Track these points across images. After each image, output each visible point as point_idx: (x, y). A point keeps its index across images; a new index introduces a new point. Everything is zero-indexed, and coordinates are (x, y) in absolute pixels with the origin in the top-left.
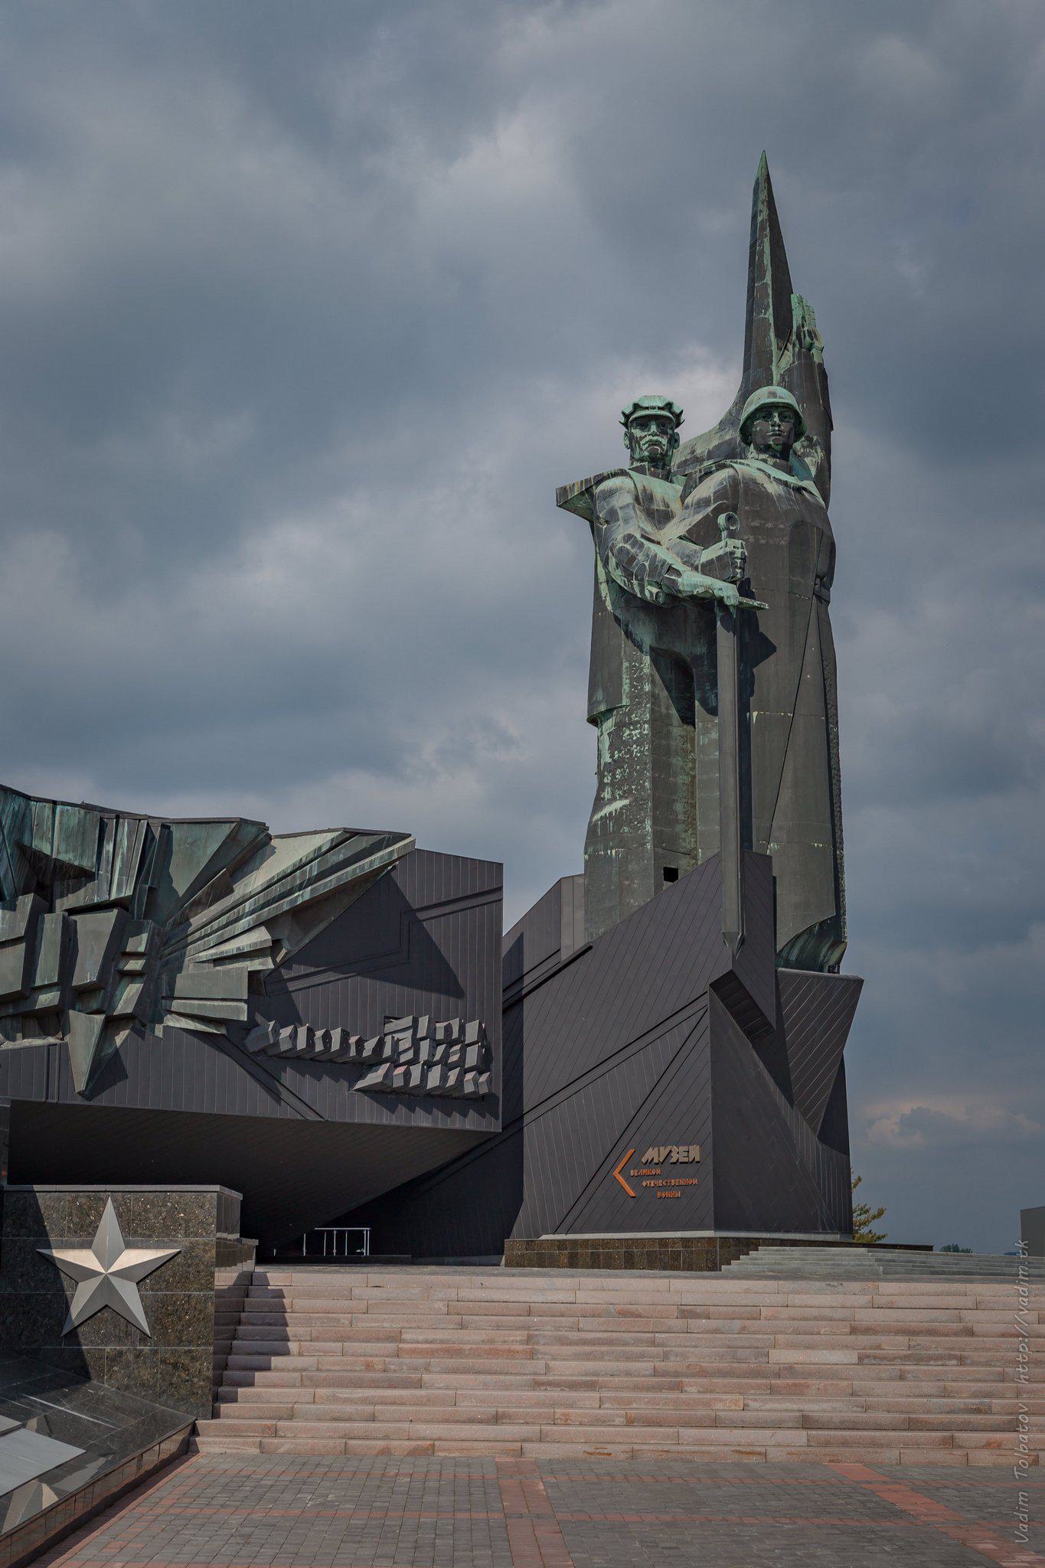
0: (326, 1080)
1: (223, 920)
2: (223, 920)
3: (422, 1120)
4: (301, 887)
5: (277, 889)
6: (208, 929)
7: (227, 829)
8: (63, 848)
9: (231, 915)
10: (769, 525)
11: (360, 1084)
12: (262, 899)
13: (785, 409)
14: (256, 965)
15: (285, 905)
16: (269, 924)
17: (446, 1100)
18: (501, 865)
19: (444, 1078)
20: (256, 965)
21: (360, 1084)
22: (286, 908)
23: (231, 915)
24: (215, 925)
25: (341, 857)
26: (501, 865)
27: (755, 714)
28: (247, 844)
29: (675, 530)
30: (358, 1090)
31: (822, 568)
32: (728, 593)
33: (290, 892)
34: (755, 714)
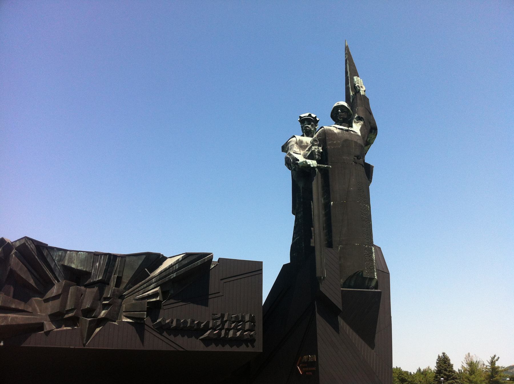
0: (186, 337)
1: (145, 285)
2: (145, 285)
3: (227, 348)
4: (173, 273)
5: (164, 274)
6: (140, 289)
7: (144, 256)
8: (79, 265)
9: (148, 284)
10: (335, 142)
11: (201, 338)
12: (158, 277)
15: (167, 279)
16: (161, 286)
17: (237, 341)
18: (262, 262)
19: (235, 333)
21: (201, 338)
22: (167, 280)
23: (148, 284)
24: (142, 287)
25: (186, 262)
26: (262, 262)
27: (332, 203)
28: (154, 260)
30: (202, 340)
31: (358, 153)
32: (313, 163)
33: (169, 274)
34: (332, 203)
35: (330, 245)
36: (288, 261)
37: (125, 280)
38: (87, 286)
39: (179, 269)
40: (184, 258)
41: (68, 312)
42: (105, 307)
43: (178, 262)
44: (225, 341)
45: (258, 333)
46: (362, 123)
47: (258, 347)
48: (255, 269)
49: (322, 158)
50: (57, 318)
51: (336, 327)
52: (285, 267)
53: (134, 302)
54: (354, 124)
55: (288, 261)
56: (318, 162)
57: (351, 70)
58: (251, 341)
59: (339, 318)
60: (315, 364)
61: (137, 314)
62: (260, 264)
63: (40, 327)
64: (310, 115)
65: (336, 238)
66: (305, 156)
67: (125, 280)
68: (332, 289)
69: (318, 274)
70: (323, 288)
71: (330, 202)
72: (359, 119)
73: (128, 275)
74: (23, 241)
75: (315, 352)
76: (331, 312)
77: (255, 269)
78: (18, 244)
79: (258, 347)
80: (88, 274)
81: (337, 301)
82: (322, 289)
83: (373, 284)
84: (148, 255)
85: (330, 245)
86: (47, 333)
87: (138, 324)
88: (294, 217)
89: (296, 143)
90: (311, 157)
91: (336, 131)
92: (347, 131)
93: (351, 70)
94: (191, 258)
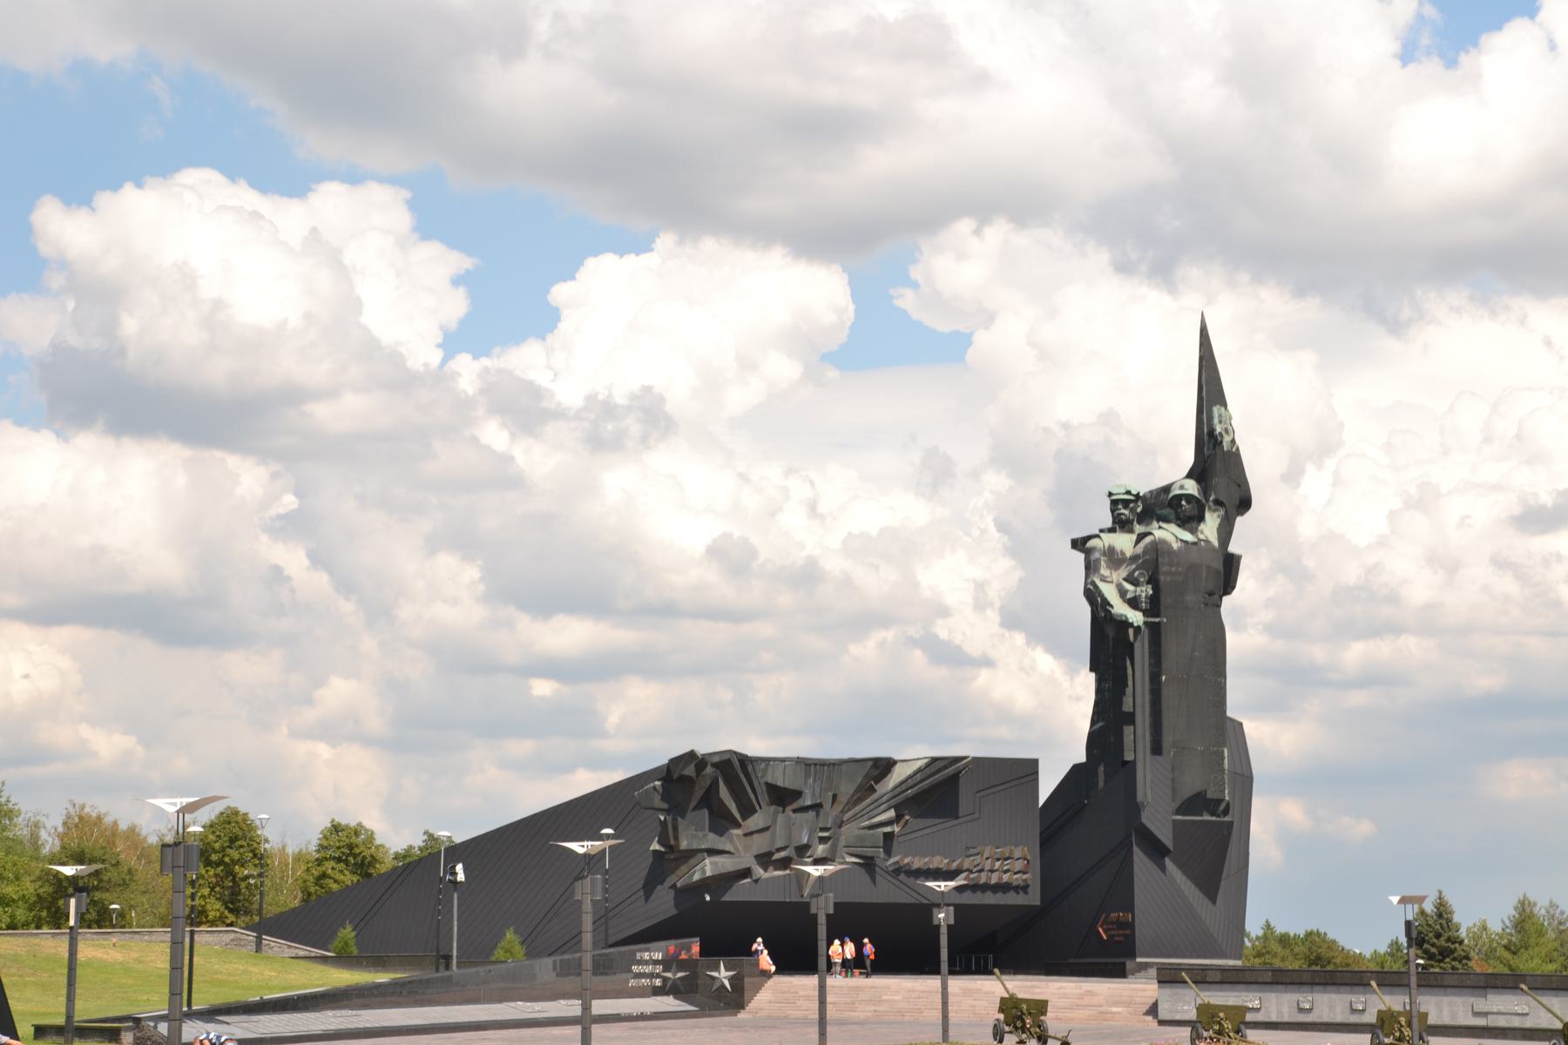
13: (1189, 498)
14: (888, 829)
16: (896, 807)
17: (1003, 888)
20: (888, 829)
28: (883, 766)
29: (1119, 575)
32: (1136, 617)
35: (1157, 749)
36: (1083, 759)
37: (843, 799)
38: (794, 811)
39: (922, 781)
40: (928, 765)
41: (779, 850)
42: (823, 840)
43: (919, 770)
44: (986, 887)
45: (1033, 877)
46: (1222, 512)
47: (1034, 898)
48: (1027, 770)
49: (1153, 607)
50: (765, 859)
51: (1163, 869)
52: (1076, 769)
53: (857, 832)
54: (1208, 515)
55: (1083, 759)
56: (1145, 613)
57: (1210, 391)
58: (1024, 888)
59: (1167, 860)
60: (1130, 926)
61: (869, 852)
62: (1035, 763)
63: (746, 873)
64: (1128, 493)
65: (1168, 739)
66: (1122, 593)
67: (843, 799)
68: (1159, 818)
69: (1140, 797)
70: (1147, 819)
71: (1160, 675)
72: (1218, 503)
73: (847, 789)
74: (726, 757)
75: (1129, 906)
76: (1157, 851)
77: (1027, 770)
78: (716, 759)
79: (1034, 898)
80: (798, 794)
81: (1166, 837)
82: (1144, 820)
83: (1222, 806)
84: (877, 762)
85: (1157, 749)
86: (756, 881)
87: (868, 864)
88: (1093, 675)
89: (1104, 554)
90: (1133, 603)
91: (1175, 546)
92: (1194, 544)
93: (1210, 391)
94: (939, 765)
